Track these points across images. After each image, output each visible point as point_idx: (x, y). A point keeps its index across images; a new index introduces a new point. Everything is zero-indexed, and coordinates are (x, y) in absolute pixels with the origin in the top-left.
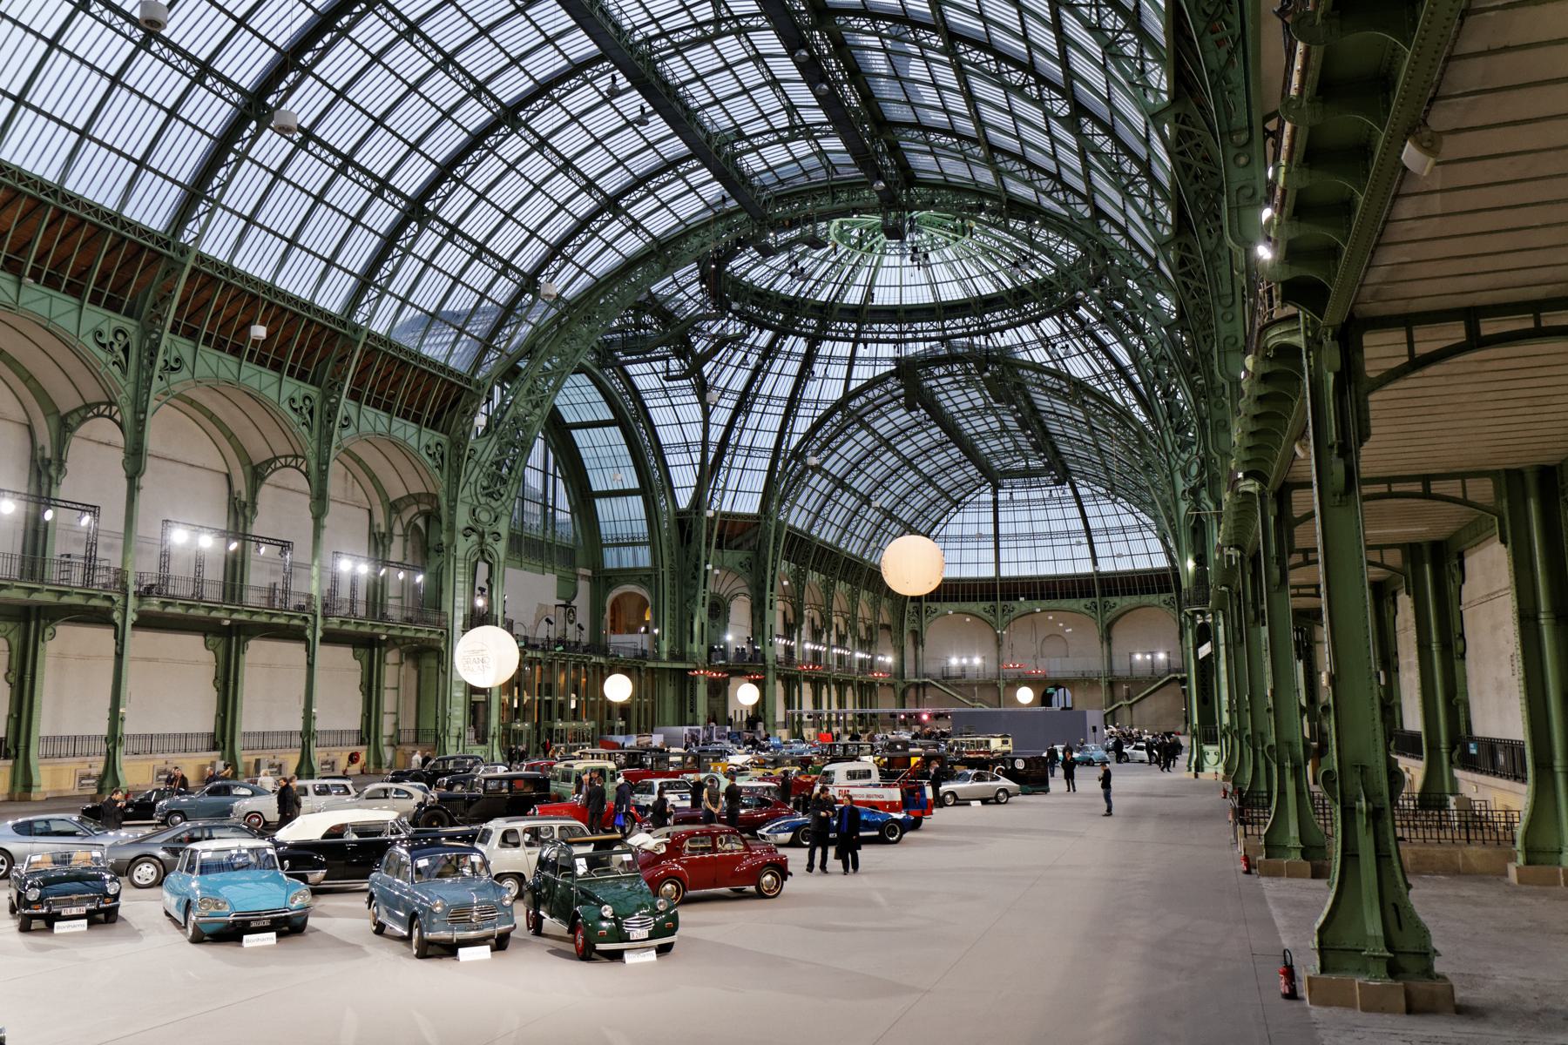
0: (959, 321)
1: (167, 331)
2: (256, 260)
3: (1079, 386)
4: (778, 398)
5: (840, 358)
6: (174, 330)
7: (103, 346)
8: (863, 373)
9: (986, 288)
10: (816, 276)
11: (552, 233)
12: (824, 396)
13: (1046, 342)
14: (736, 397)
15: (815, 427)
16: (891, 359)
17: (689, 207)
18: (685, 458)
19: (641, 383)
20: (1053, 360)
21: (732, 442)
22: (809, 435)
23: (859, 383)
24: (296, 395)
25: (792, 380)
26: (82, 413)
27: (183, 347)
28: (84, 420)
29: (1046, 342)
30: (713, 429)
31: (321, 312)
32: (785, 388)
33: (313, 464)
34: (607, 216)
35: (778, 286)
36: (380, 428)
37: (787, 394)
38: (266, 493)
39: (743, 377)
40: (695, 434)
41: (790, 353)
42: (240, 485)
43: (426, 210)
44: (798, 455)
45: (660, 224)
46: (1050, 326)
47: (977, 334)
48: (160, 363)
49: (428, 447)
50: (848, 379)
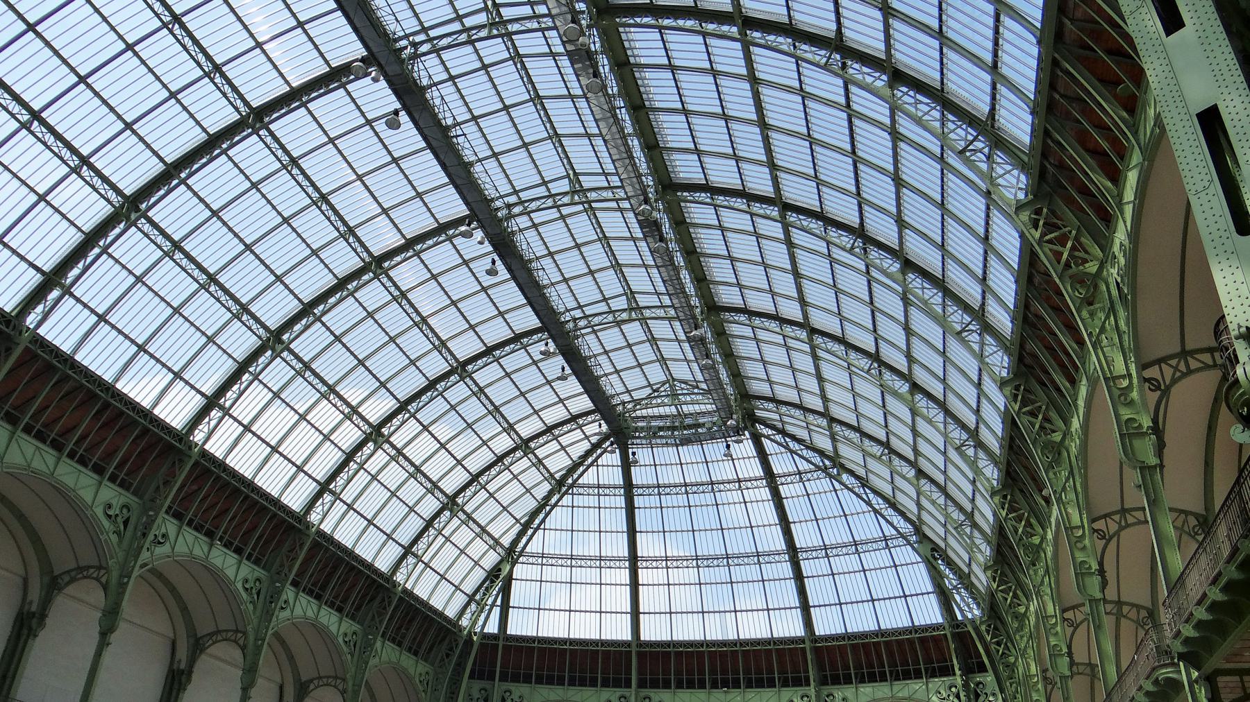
1: (162, 514)
2: (244, 461)
6: (167, 512)
7: (110, 516)
11: (475, 464)
24: (250, 577)
26: (73, 574)
27: (171, 526)
28: (73, 580)
31: (285, 508)
33: (251, 638)
34: (519, 454)
36: (310, 613)
38: (204, 662)
42: (182, 654)
43: (382, 435)
48: (151, 537)
49: (346, 635)
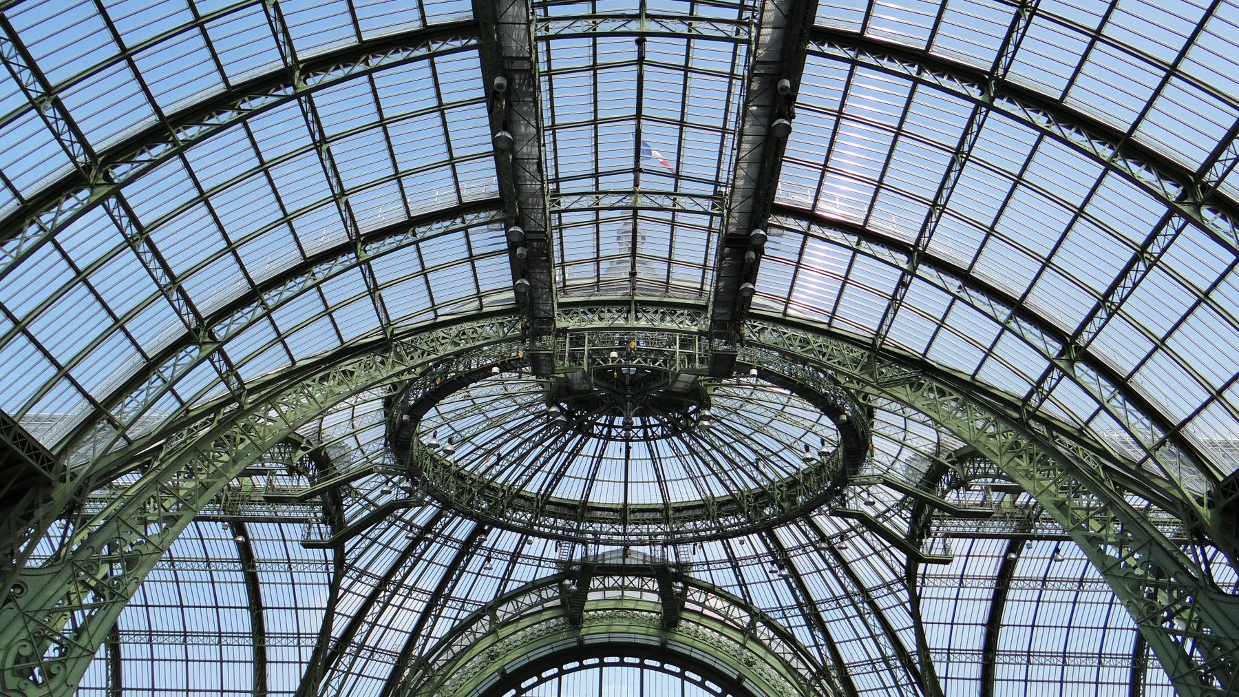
0: (644, 528)
3: (759, 616)
4: (420, 591)
5: (502, 552)
8: (524, 573)
9: (682, 493)
10: (503, 451)
12: (472, 597)
13: (734, 562)
14: (374, 582)
15: (455, 632)
16: (557, 562)
17: (454, 288)
18: (292, 654)
19: (260, 551)
20: (740, 586)
21: (357, 639)
22: (446, 641)
23: (516, 585)
25: (442, 571)
29: (734, 562)
30: (337, 618)
32: (430, 582)
35: (459, 453)
37: (432, 587)
39: (389, 558)
40: (313, 623)
41: (448, 538)
44: (423, 662)
45: (406, 304)
46: (741, 547)
47: (665, 544)
50: (505, 580)
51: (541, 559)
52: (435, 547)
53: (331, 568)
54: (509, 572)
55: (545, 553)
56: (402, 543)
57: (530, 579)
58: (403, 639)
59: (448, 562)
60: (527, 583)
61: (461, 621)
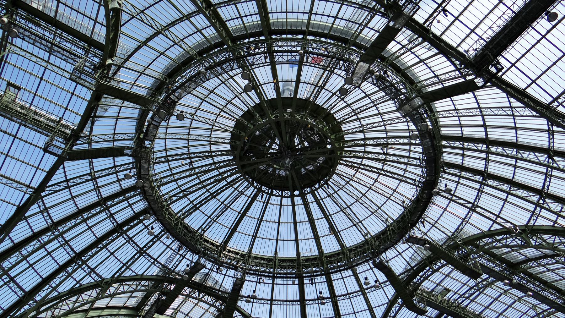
8: (141, 266)
12: (98, 270)
15: (73, 292)
25: (92, 239)
37: (78, 249)
51: (155, 260)
52: (103, 215)
53: (30, 191)
54: (133, 260)
55: (167, 253)
56: (82, 203)
57: (140, 273)
58: (37, 280)
59: (99, 235)
60: (137, 275)
61: (81, 285)
